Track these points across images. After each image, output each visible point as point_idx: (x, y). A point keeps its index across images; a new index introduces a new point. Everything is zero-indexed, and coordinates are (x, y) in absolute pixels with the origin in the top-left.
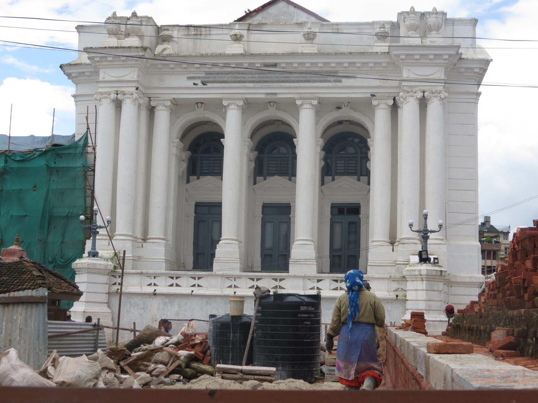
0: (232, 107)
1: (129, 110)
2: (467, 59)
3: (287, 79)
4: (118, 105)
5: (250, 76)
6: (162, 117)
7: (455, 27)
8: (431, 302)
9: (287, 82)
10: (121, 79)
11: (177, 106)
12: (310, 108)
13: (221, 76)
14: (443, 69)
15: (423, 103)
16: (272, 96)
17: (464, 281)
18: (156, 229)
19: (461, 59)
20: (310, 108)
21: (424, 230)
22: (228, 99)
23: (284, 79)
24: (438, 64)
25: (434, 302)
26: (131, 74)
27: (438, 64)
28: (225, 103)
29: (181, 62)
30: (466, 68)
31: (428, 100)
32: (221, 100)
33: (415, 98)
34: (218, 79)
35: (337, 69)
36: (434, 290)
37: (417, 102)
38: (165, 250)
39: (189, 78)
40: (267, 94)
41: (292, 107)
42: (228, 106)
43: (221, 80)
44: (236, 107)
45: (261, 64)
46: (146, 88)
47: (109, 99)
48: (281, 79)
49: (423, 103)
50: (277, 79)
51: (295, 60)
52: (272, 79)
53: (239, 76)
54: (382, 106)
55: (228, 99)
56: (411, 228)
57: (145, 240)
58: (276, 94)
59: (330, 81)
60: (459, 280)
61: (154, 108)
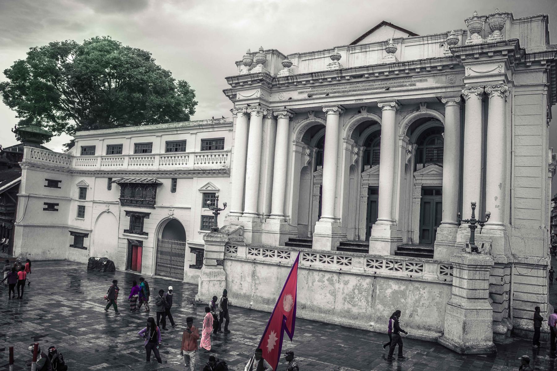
0: (330, 112)
1: (255, 120)
3: (370, 87)
4: (248, 116)
5: (343, 87)
6: (283, 123)
9: (371, 89)
10: (249, 98)
11: (295, 115)
12: (389, 110)
14: (503, 64)
15: (485, 98)
18: (277, 209)
20: (389, 110)
21: (471, 220)
22: (326, 107)
23: (368, 87)
26: (256, 93)
28: (324, 110)
29: (292, 82)
31: (489, 94)
32: (321, 107)
34: (320, 92)
42: (327, 112)
44: (333, 113)
45: (351, 76)
46: (271, 103)
48: (367, 87)
49: (485, 98)
50: (364, 88)
52: (360, 88)
55: (326, 107)
57: (269, 216)
59: (406, 86)
61: (277, 116)
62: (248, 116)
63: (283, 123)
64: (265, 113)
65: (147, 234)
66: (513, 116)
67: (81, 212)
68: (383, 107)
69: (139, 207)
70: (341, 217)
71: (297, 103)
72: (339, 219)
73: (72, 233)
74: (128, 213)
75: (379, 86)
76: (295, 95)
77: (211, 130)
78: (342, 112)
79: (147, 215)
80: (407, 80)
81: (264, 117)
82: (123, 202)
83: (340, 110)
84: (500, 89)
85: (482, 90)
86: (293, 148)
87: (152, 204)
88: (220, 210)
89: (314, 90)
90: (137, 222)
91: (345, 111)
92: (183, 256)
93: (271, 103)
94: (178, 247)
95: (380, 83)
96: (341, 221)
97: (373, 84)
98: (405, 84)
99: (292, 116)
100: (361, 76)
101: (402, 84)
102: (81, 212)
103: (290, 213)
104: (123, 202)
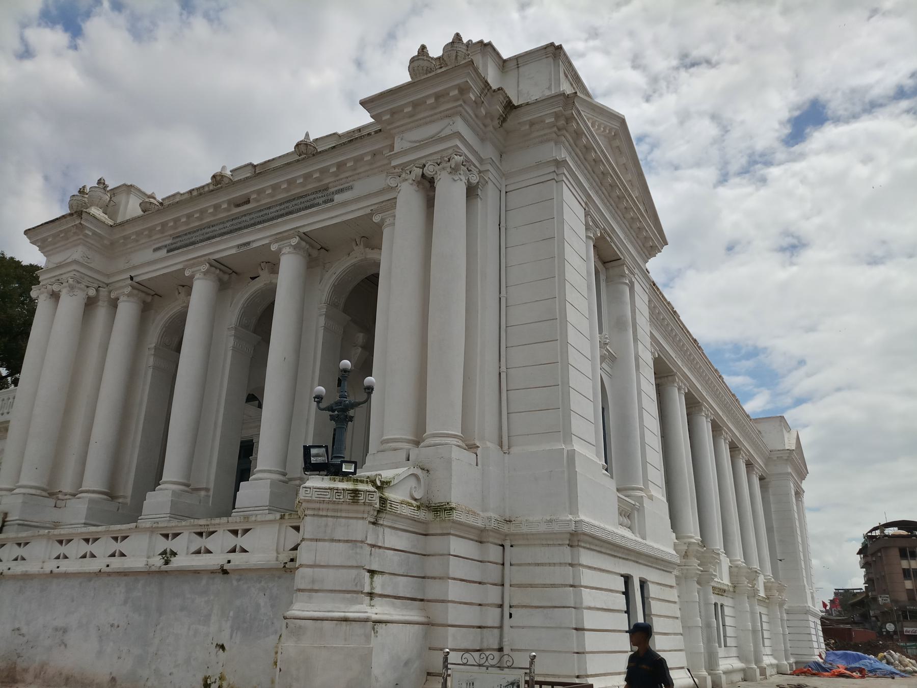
2: (528, 104)
3: (265, 218)
5: (221, 226)
7: (520, 69)
8: (316, 570)
9: (264, 221)
11: (150, 296)
13: (189, 236)
16: (245, 248)
17: (534, 531)
19: (510, 107)
24: (446, 113)
25: (331, 571)
27: (446, 113)
30: (532, 124)
32: (184, 269)
33: (410, 181)
35: (326, 181)
36: (332, 540)
37: (415, 187)
38: (89, 509)
39: (155, 250)
40: (239, 246)
42: (192, 278)
43: (188, 242)
45: (229, 202)
46: (108, 276)
47: (46, 294)
48: (259, 219)
50: (252, 222)
51: (266, 183)
53: (209, 230)
54: (388, 222)
56: (318, 402)
58: (248, 243)
59: (318, 204)
60: (525, 529)
62: (55, 296)
63: (127, 310)
64: (92, 292)
66: (503, 230)
68: (280, 250)
70: (211, 486)
71: (146, 270)
72: (207, 490)
75: (276, 214)
76: (148, 255)
78: (226, 277)
80: (320, 195)
81: (90, 304)
83: (218, 271)
84: (449, 164)
85: (419, 171)
86: (149, 360)
89: (175, 241)
91: (227, 275)
93: (108, 276)
95: (278, 208)
96: (211, 493)
97: (267, 212)
98: (316, 201)
99: (149, 299)
101: (311, 203)
103: (127, 489)
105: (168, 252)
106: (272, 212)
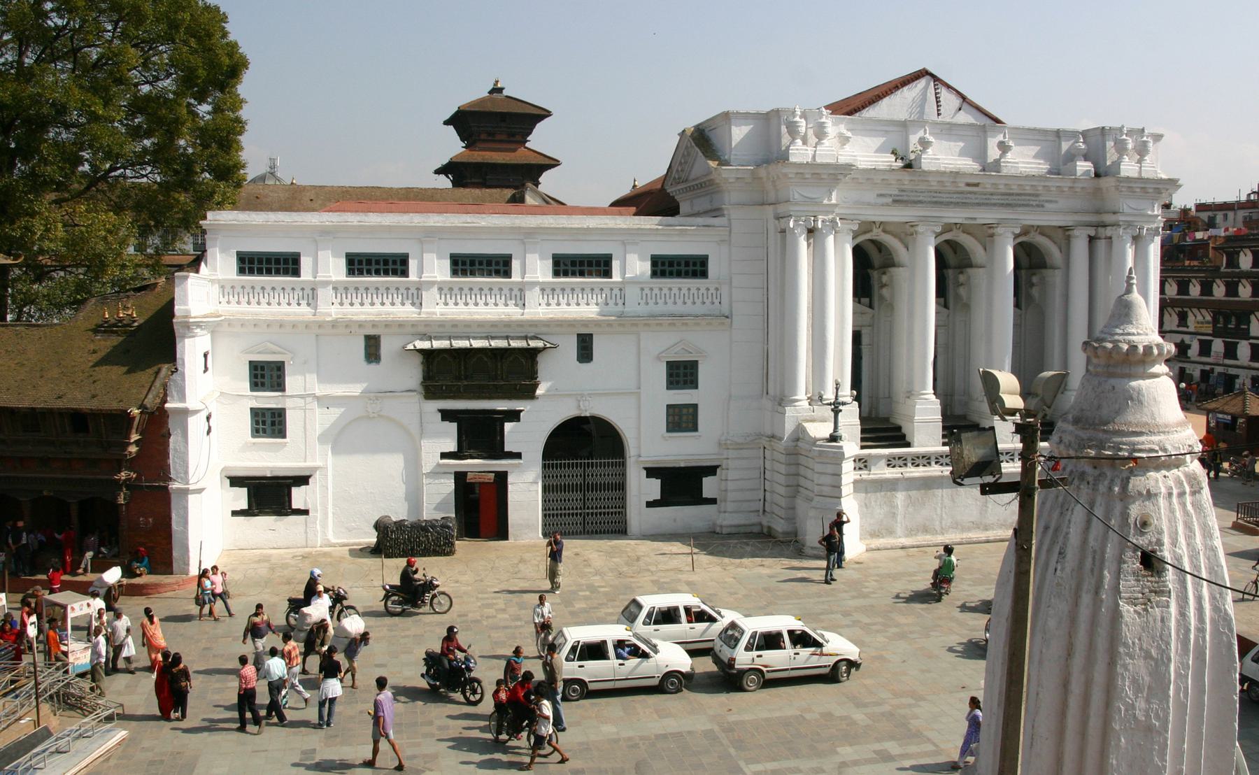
41: (987, 234)
65: (518, 456)
67: (269, 423)
69: (490, 398)
73: (236, 481)
74: (447, 415)
77: (676, 238)
79: (514, 416)
82: (431, 389)
87: (528, 392)
88: (844, 404)
90: (480, 435)
92: (621, 487)
94: (610, 470)
100: (977, 185)
102: (269, 423)
104: (431, 389)
105: (895, 201)
106: (995, 199)
